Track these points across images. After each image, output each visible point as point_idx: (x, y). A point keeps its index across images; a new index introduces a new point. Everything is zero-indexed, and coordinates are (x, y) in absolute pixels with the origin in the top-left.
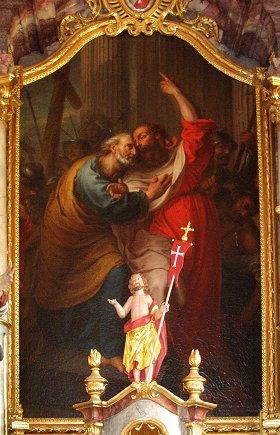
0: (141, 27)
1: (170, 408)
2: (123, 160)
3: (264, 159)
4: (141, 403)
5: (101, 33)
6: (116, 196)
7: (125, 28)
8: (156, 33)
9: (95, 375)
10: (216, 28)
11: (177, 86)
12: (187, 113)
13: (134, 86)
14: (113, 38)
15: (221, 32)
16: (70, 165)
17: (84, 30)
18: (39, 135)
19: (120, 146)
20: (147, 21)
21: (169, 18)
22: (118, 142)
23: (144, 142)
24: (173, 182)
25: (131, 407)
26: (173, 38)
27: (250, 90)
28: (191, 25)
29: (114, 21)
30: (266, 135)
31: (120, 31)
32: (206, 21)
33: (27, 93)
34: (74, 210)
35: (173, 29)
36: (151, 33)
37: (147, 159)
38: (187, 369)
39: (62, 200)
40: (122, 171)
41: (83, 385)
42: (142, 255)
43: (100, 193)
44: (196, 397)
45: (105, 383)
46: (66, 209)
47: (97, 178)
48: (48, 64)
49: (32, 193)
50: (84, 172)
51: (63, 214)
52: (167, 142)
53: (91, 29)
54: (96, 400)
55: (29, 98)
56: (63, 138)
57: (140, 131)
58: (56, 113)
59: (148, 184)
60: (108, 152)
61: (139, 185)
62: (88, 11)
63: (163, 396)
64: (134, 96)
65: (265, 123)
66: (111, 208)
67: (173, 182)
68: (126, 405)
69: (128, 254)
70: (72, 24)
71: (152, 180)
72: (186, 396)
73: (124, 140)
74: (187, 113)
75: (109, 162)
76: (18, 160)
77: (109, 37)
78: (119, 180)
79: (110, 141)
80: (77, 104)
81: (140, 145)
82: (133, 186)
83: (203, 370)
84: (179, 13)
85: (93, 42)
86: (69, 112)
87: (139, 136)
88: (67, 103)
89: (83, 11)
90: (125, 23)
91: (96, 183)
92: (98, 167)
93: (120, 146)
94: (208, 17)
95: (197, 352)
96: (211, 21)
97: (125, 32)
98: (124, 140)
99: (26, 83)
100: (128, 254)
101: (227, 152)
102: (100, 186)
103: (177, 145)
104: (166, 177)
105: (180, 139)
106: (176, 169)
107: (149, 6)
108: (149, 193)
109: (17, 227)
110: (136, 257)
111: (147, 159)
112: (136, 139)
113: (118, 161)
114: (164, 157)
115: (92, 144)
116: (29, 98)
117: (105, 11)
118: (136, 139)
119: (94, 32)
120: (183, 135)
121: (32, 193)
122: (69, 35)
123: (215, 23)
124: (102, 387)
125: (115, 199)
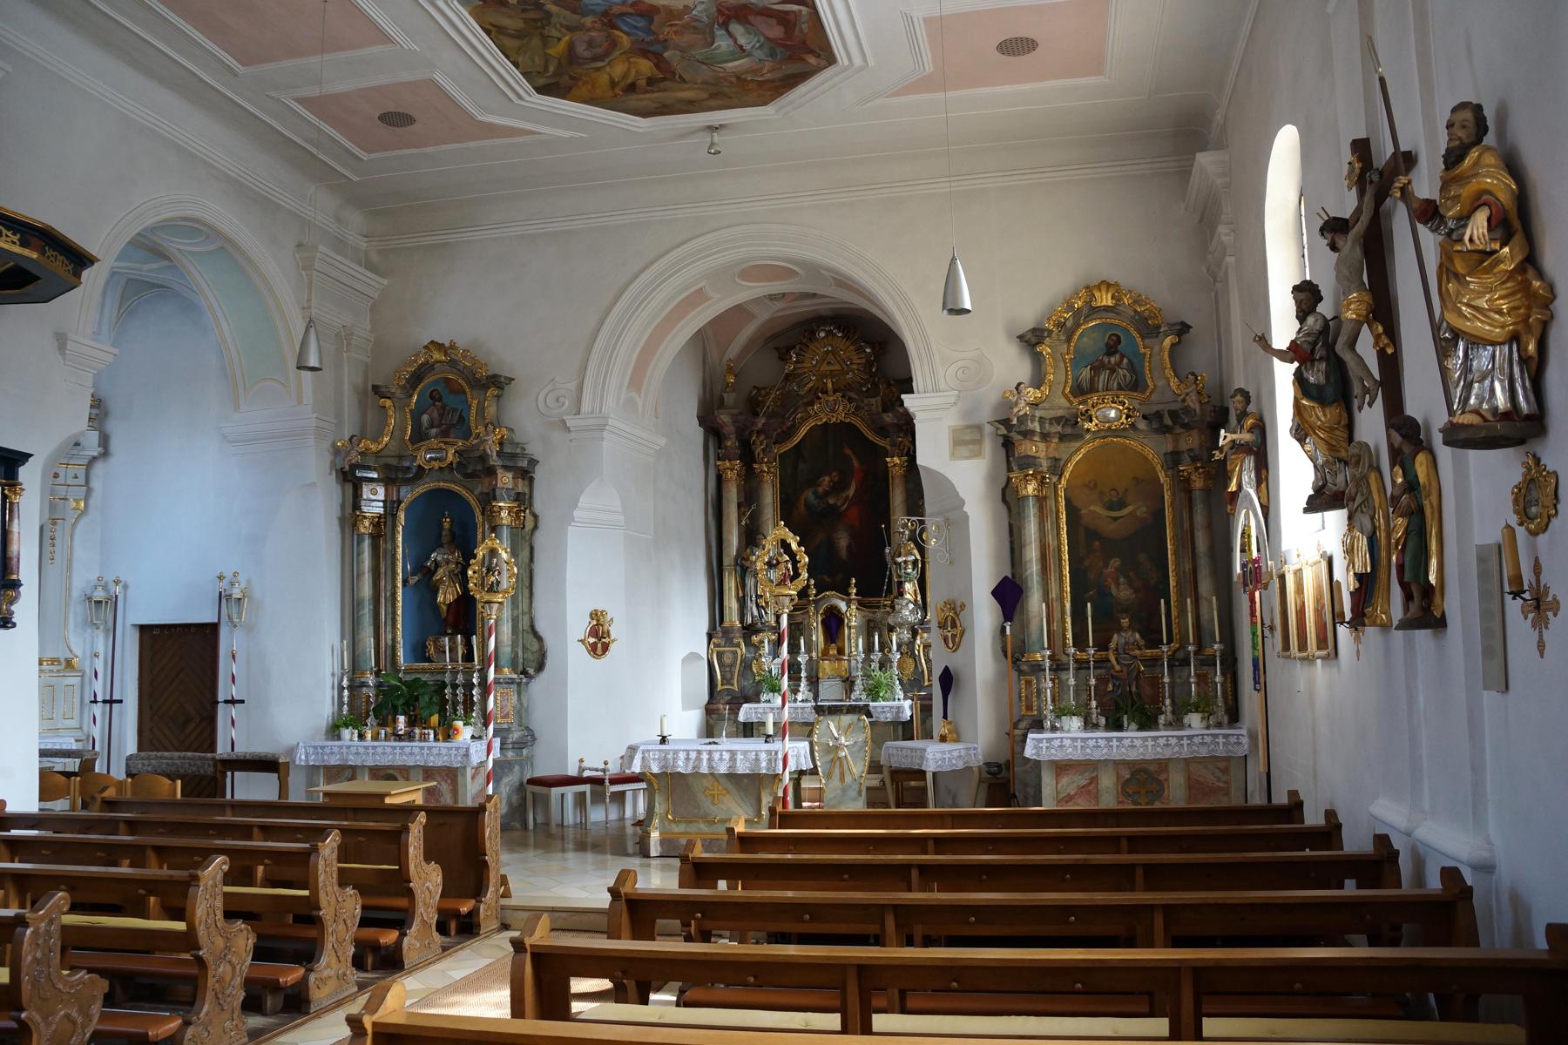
12: (856, 463)
38: (849, 585)
40: (827, 494)
50: (809, 495)
72: (849, 595)
73: (827, 479)
74: (856, 463)
75: (820, 490)
82: (831, 501)
86: (802, 466)
92: (815, 493)
98: (827, 479)
106: (851, 492)
114: (846, 486)
115: (812, 482)
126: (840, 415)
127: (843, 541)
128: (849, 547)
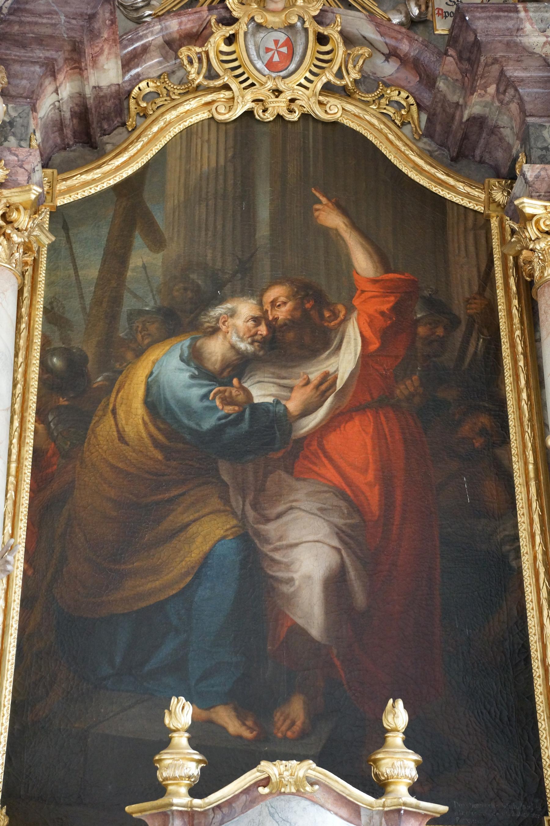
0: (278, 106)
1: (344, 812)
2: (243, 346)
3: (513, 346)
4: (279, 802)
5: (204, 115)
6: (229, 409)
7: (249, 105)
8: (305, 117)
9: (178, 747)
10: (414, 108)
11: (343, 211)
12: (363, 263)
13: (264, 213)
14: (226, 123)
15: (424, 117)
16: (139, 353)
17: (174, 107)
18: (82, 297)
19: (238, 321)
20: (288, 95)
21: (328, 88)
22: (233, 314)
23: (282, 314)
24: (339, 384)
25: (257, 808)
26: (335, 124)
27: (481, 222)
28: (367, 103)
29: (228, 94)
30: (515, 302)
31: (239, 111)
32: (394, 95)
33: (63, 220)
34: (144, 435)
35: (335, 110)
36: (295, 117)
37: (291, 343)
38: (379, 737)
39: (121, 413)
40: (240, 366)
41: (152, 769)
42: (279, 516)
43: (197, 404)
44: (400, 794)
45: (199, 762)
46: (130, 431)
47: (193, 377)
48: (106, 168)
49: (63, 401)
50: (168, 366)
51: (121, 438)
52: (327, 314)
53: (186, 107)
54: (180, 798)
55: (66, 228)
56: (129, 303)
57: (277, 292)
58: (117, 258)
59: (291, 389)
60: (214, 331)
61: (274, 390)
62: (180, 74)
63: (328, 789)
64: (263, 230)
65: (512, 281)
66: (218, 430)
67: (339, 384)
68: (246, 808)
69: (251, 514)
70: (151, 97)
71: (299, 382)
72: (377, 788)
75: (216, 349)
76: (37, 341)
77: (219, 123)
78: (235, 381)
79: (219, 311)
80: (157, 242)
81: (276, 319)
82: (262, 391)
83: (411, 740)
84: (347, 81)
85: (189, 129)
86: (141, 256)
87: (273, 303)
88: (138, 241)
89: (173, 72)
90: (250, 95)
91: (190, 386)
92: (195, 358)
93: (238, 321)
94: (400, 87)
95: (400, 703)
96: (404, 94)
97: (249, 113)
98: (245, 309)
99: (60, 202)
100: (251, 514)
101: (440, 332)
102: (197, 392)
103: (346, 320)
104: (326, 376)
105: (350, 309)
106: (344, 362)
107: (292, 67)
108: (293, 406)
109: (28, 463)
110: (268, 520)
111: (291, 343)
112: (267, 307)
113: (233, 347)
115: (183, 316)
116: (66, 228)
117: (212, 75)
118: (267, 307)
119: (191, 112)
120: (356, 302)
121: (63, 401)
122: (145, 116)
123: (411, 100)
124: (193, 769)
125: (228, 415)
126: (298, 93)
127: (308, 555)
128: (336, 584)
